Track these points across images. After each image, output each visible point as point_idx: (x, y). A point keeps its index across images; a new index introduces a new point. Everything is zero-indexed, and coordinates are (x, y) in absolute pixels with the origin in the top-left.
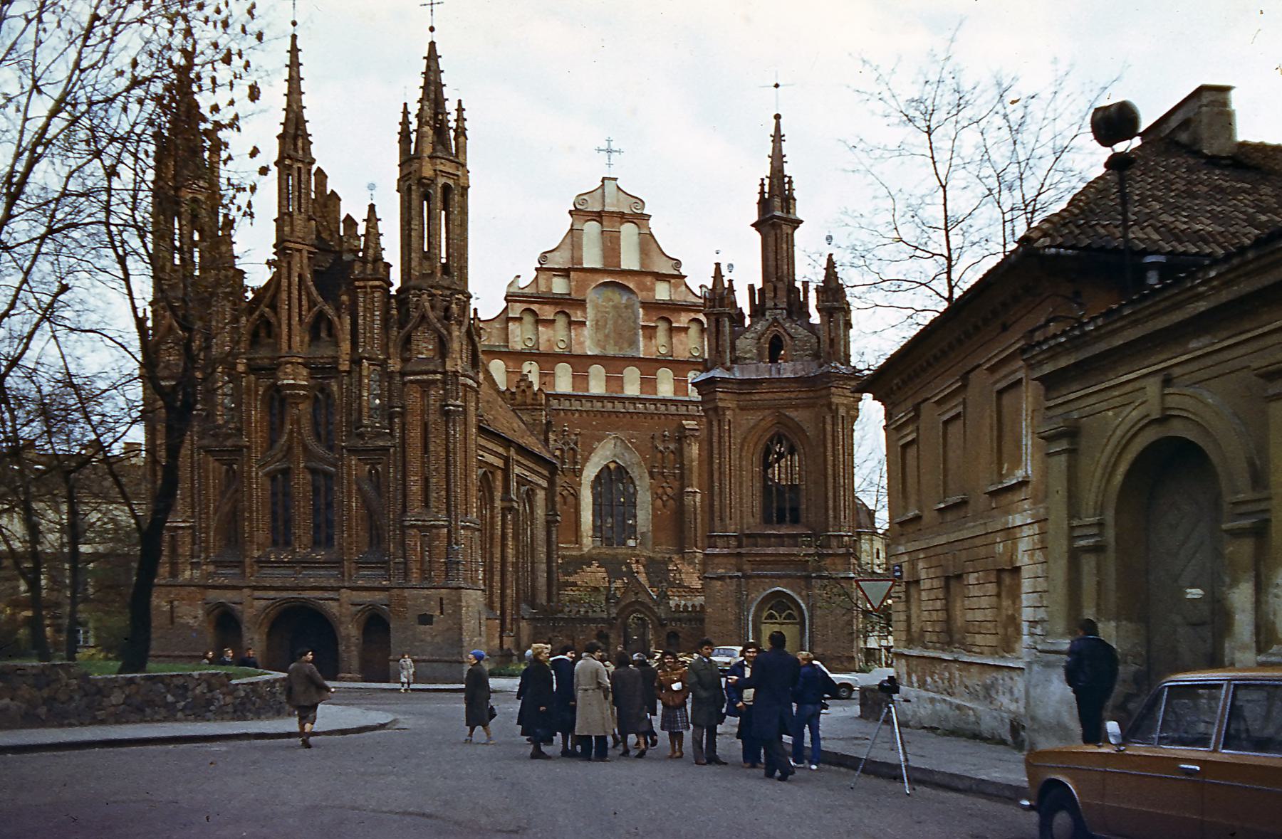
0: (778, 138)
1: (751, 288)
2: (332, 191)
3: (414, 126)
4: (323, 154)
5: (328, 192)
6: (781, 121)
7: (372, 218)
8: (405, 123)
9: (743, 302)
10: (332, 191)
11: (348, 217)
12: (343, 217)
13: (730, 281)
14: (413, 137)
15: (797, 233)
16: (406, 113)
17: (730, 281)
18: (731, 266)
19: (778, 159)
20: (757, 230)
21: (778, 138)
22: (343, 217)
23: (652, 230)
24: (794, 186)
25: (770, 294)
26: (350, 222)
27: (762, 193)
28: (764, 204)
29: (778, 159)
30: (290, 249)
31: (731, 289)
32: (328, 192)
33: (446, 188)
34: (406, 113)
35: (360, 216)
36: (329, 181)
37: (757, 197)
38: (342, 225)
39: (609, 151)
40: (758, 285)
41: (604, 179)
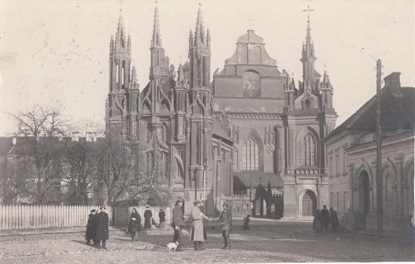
0: (309, 30)
1: (300, 82)
2: (167, 57)
3: (194, 36)
4: (164, 45)
8: (191, 35)
9: (297, 87)
10: (167, 57)
11: (172, 65)
12: (170, 65)
13: (293, 79)
14: (194, 40)
15: (315, 62)
17: (293, 79)
18: (293, 74)
19: (308, 38)
20: (302, 61)
21: (309, 30)
22: (170, 65)
25: (305, 85)
27: (303, 48)
28: (304, 53)
29: (308, 38)
30: (156, 78)
31: (293, 82)
33: (204, 57)
37: (302, 50)
40: (302, 81)
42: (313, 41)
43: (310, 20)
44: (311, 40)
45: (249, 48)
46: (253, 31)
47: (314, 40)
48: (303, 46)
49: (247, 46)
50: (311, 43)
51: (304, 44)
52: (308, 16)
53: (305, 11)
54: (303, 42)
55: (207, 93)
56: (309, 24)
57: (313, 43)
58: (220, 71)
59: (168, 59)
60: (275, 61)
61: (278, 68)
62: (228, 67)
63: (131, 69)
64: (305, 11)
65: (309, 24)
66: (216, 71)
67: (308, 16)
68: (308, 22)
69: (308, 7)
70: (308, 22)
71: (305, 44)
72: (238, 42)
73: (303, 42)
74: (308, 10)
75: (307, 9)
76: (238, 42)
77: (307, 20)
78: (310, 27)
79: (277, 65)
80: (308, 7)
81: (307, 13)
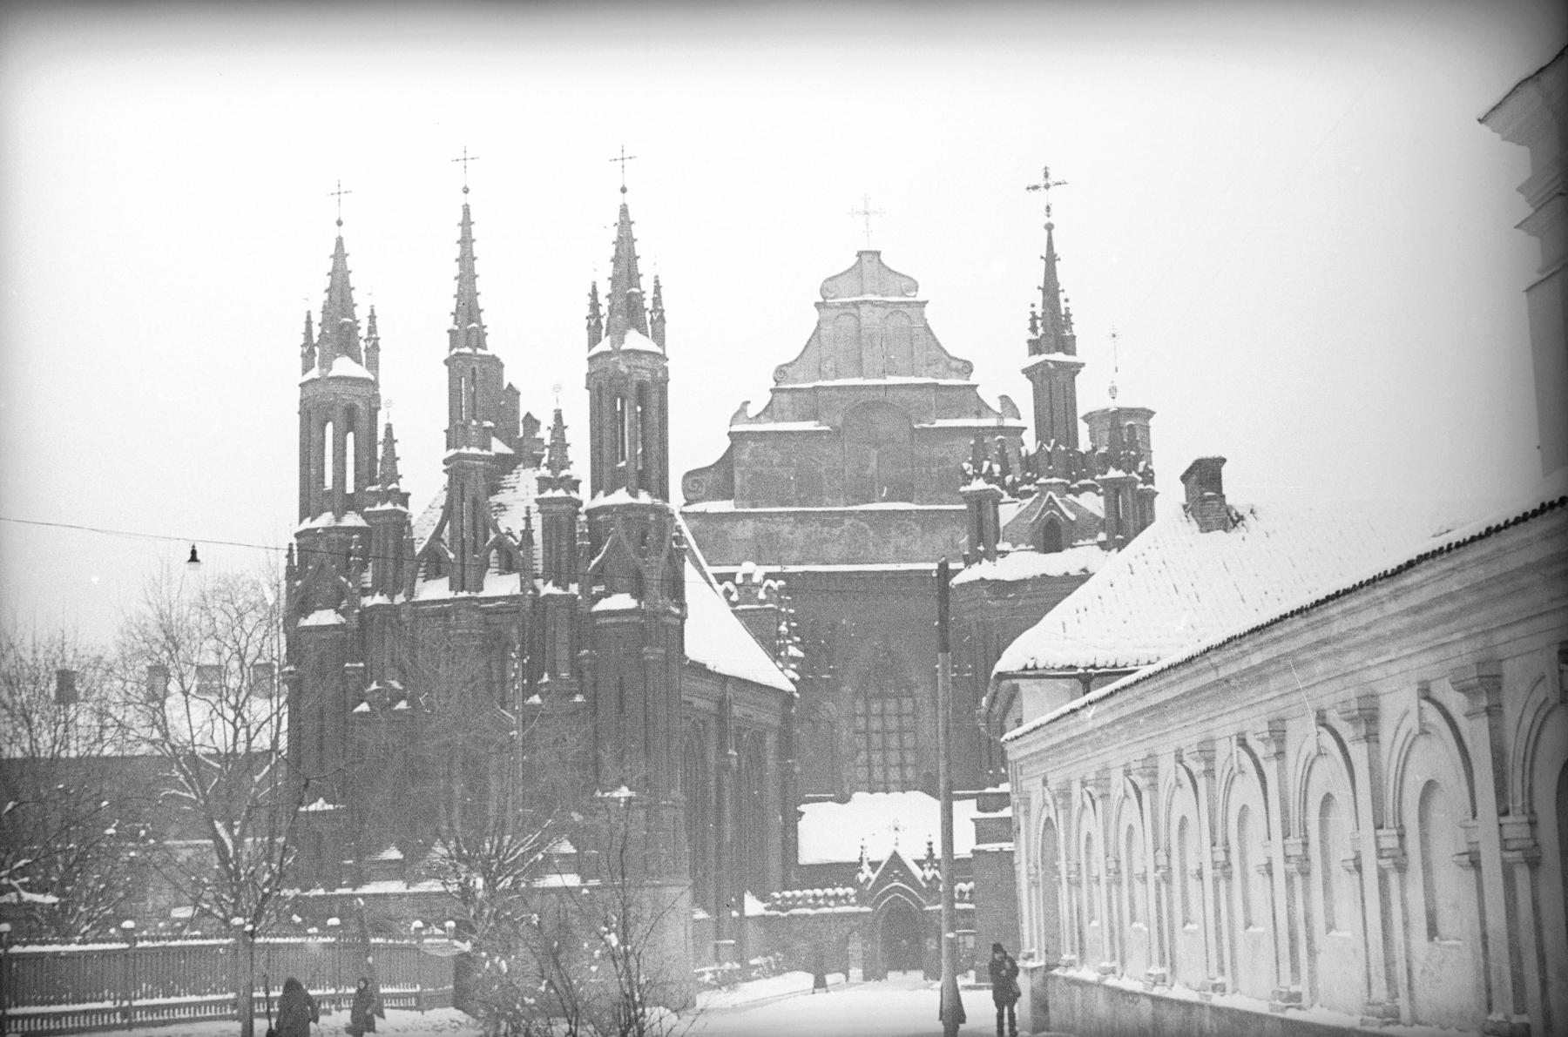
0: (1051, 259)
2: (510, 385)
3: (604, 310)
5: (505, 385)
6: (1053, 231)
7: (559, 426)
12: (522, 415)
16: (594, 294)
19: (1051, 289)
21: (1051, 259)
22: (522, 415)
23: (928, 322)
24: (1073, 319)
26: (532, 423)
29: (1051, 289)
32: (505, 385)
33: (642, 388)
34: (594, 294)
35: (547, 421)
36: (506, 370)
38: (521, 426)
39: (866, 213)
41: (860, 254)
42: (1067, 300)
43: (1051, 220)
44: (1062, 297)
45: (864, 321)
46: (878, 253)
47: (1073, 298)
48: (1034, 318)
49: (854, 311)
50: (1063, 305)
51: (1033, 313)
52: (1048, 208)
53: (1036, 188)
54: (1033, 305)
55: (652, 517)
56: (1050, 237)
57: (1067, 309)
58: (752, 411)
59: (513, 393)
60: (967, 368)
61: (978, 390)
62: (786, 398)
63: (381, 436)
64: (1036, 188)
65: (1050, 237)
66: (735, 419)
67: (1048, 208)
68: (1049, 227)
69: (1046, 175)
70: (1049, 227)
71: (1039, 314)
72: (821, 300)
73: (1033, 305)
74: (1047, 187)
75: (1042, 183)
76: (821, 300)
77: (1047, 220)
78: (1056, 250)
79: (972, 381)
80: (1046, 175)
81: (1042, 197)
